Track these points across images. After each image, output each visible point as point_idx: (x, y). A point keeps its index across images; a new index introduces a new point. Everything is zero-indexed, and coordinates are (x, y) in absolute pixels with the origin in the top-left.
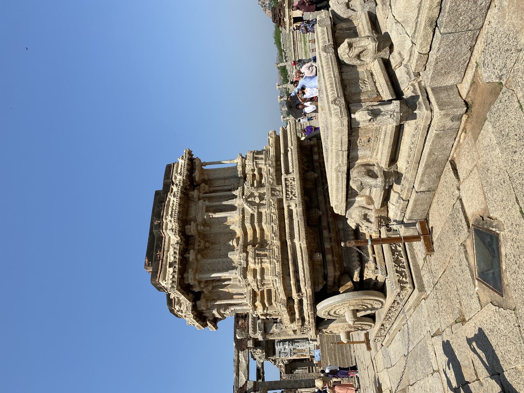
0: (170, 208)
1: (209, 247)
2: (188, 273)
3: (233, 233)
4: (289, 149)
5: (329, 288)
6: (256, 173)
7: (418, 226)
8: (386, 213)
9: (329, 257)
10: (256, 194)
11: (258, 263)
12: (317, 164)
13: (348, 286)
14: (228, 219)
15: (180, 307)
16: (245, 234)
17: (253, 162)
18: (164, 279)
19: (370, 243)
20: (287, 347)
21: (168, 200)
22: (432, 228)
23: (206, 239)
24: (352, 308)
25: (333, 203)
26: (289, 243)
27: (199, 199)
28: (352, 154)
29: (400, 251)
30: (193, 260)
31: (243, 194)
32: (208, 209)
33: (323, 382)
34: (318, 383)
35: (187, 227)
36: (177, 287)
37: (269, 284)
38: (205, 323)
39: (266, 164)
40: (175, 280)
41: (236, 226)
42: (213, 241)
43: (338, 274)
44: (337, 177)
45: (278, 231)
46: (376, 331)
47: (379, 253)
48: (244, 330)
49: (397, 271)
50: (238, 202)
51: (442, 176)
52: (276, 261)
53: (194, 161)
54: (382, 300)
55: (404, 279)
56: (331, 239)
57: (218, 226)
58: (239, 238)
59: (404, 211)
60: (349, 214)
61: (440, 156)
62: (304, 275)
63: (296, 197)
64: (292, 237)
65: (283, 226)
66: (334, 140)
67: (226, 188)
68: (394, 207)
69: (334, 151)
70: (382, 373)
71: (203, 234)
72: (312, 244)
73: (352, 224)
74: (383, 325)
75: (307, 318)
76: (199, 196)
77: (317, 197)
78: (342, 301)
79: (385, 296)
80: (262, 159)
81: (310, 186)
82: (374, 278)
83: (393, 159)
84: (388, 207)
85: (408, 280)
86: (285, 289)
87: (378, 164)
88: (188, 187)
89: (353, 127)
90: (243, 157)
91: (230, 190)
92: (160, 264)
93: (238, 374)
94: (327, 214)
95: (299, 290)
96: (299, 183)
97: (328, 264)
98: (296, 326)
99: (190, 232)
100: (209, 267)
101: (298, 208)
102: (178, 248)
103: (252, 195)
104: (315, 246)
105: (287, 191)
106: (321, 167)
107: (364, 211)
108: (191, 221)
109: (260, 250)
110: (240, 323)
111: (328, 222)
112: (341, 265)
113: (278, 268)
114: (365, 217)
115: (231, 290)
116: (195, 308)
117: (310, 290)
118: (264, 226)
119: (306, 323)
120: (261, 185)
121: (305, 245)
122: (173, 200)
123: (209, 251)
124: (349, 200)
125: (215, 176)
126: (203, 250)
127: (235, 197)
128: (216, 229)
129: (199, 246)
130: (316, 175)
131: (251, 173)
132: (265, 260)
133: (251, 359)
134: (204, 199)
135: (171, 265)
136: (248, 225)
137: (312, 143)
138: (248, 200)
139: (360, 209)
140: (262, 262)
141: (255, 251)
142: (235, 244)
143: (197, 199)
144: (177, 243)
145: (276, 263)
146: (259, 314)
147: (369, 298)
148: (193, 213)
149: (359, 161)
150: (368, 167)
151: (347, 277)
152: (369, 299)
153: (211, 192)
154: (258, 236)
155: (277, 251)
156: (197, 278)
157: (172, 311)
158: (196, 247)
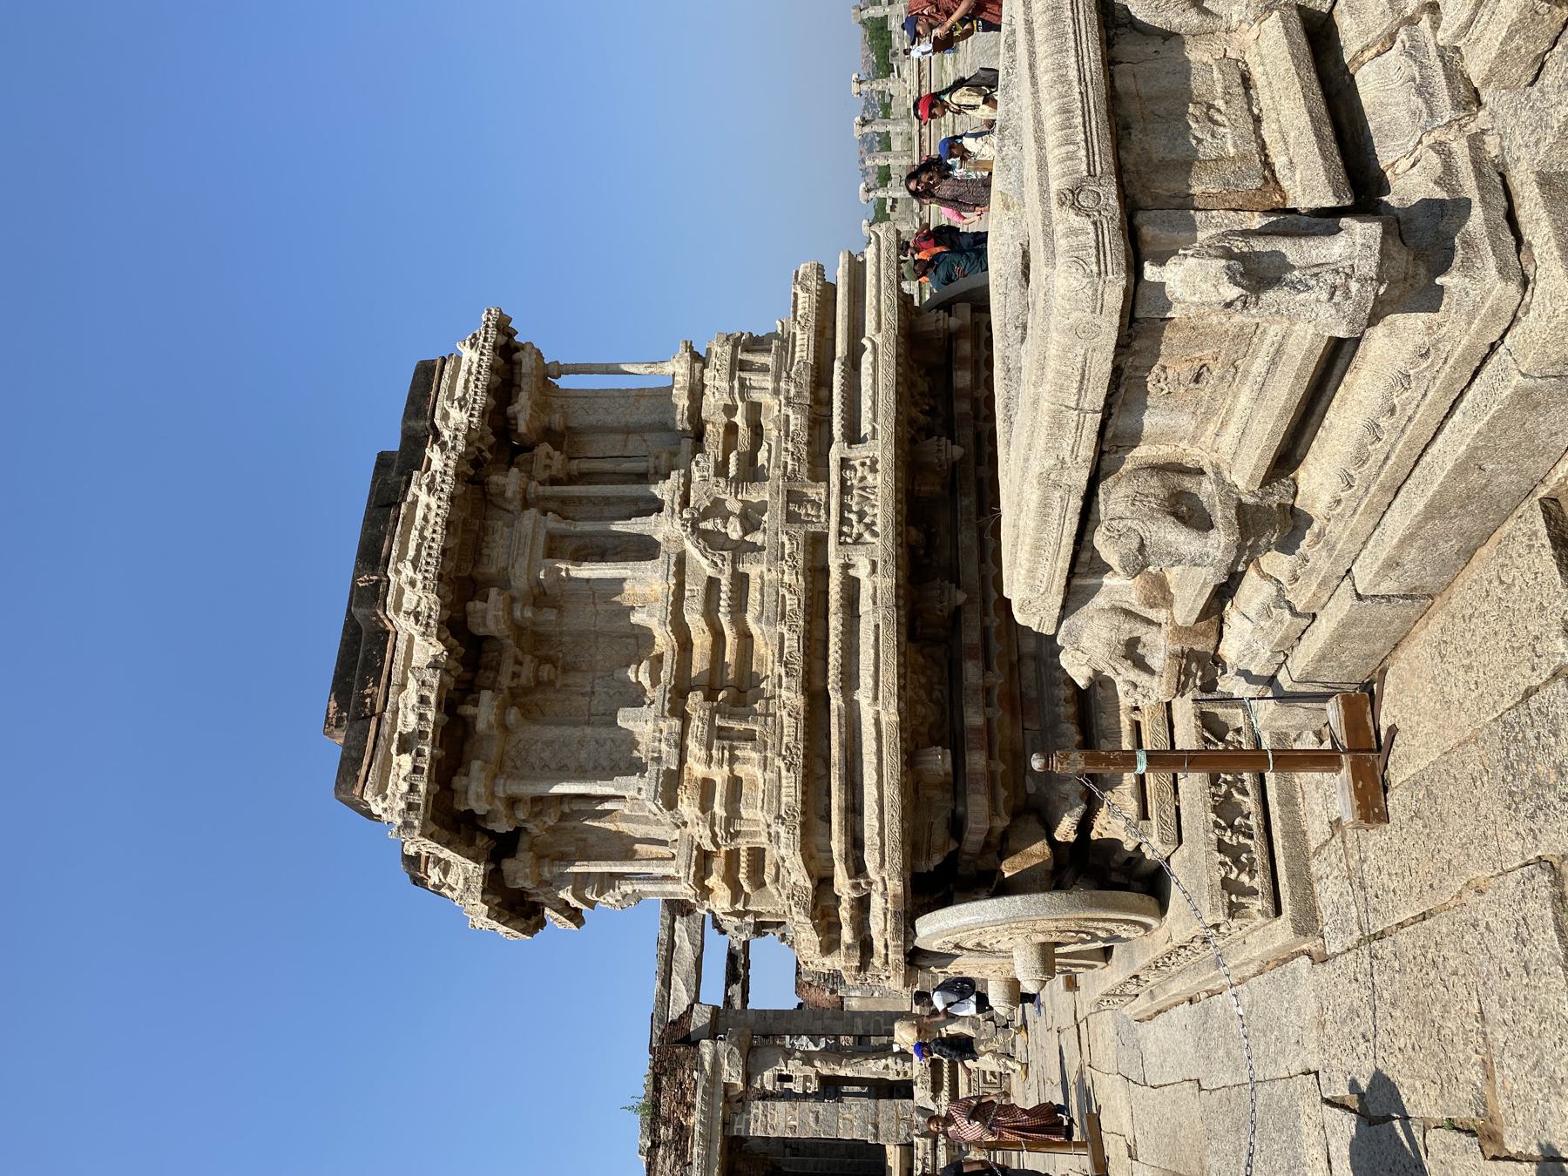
0: (415, 533)
1: (551, 683)
2: (467, 775)
3: (644, 637)
4: (864, 341)
6: (739, 419)
7: (1333, 712)
8: (1213, 642)
9: (977, 760)
10: (733, 505)
11: (721, 765)
12: (963, 406)
13: (1032, 855)
14: (627, 586)
15: (445, 872)
17: (732, 379)
18: (381, 791)
19: (1142, 767)
21: (409, 498)
22: (1393, 731)
23: (543, 652)
24: (1042, 938)
25: (1015, 587)
26: (836, 701)
27: (526, 504)
28: (1120, 422)
30: (490, 727)
31: (685, 502)
32: (555, 547)
33: (919, 1032)
34: (903, 1034)
35: (475, 606)
36: (424, 825)
37: (754, 834)
38: (533, 921)
39: (776, 392)
40: (419, 799)
42: (569, 659)
44: (1045, 504)
45: (799, 656)
49: (1222, 847)
50: (665, 528)
51: (1483, 551)
53: (517, 356)
55: (1244, 878)
56: (988, 691)
57: (590, 608)
58: (659, 659)
59: (1284, 651)
60: (1069, 633)
61: (1504, 478)
62: (882, 828)
63: (875, 534)
64: (850, 680)
66: (1052, 364)
67: (627, 466)
68: (1248, 626)
69: (1045, 405)
70: (1107, 1080)
71: (535, 633)
72: (921, 710)
73: (1076, 667)
75: (878, 945)
76: (525, 491)
77: (954, 531)
78: (1008, 921)
79: (1163, 908)
80: (764, 369)
81: (930, 487)
82: (1129, 846)
83: (1287, 459)
84: (1222, 621)
87: (1218, 473)
88: (488, 455)
89: (1140, 314)
90: (696, 357)
91: (643, 478)
92: (372, 734)
93: (666, 983)
94: (985, 601)
95: (857, 868)
96: (891, 482)
97: (970, 787)
99: (485, 625)
100: (546, 755)
101: (878, 579)
103: (717, 508)
104: (930, 722)
105: (844, 507)
106: (976, 417)
108: (490, 583)
109: (731, 716)
111: (985, 631)
114: (1132, 653)
115: (623, 827)
118: (754, 629)
119: (877, 961)
120: (752, 472)
121: (895, 718)
122: (427, 503)
125: (591, 419)
126: (527, 691)
127: (656, 506)
128: (580, 619)
129: (515, 675)
130: (957, 451)
131: (722, 419)
132: (746, 751)
133: (710, 932)
134: (544, 506)
135: (405, 745)
136: (694, 620)
137: (954, 322)
138: (703, 525)
140: (733, 759)
141: (712, 719)
142: (645, 679)
143: (516, 505)
144: (434, 665)
145: (784, 773)
147: (1104, 916)
148: (497, 556)
149: (1142, 452)
150: (1175, 478)
151: (1033, 825)
152: (1104, 920)
153: (571, 480)
154: (729, 657)
155: (790, 730)
157: (419, 882)
158: (505, 681)
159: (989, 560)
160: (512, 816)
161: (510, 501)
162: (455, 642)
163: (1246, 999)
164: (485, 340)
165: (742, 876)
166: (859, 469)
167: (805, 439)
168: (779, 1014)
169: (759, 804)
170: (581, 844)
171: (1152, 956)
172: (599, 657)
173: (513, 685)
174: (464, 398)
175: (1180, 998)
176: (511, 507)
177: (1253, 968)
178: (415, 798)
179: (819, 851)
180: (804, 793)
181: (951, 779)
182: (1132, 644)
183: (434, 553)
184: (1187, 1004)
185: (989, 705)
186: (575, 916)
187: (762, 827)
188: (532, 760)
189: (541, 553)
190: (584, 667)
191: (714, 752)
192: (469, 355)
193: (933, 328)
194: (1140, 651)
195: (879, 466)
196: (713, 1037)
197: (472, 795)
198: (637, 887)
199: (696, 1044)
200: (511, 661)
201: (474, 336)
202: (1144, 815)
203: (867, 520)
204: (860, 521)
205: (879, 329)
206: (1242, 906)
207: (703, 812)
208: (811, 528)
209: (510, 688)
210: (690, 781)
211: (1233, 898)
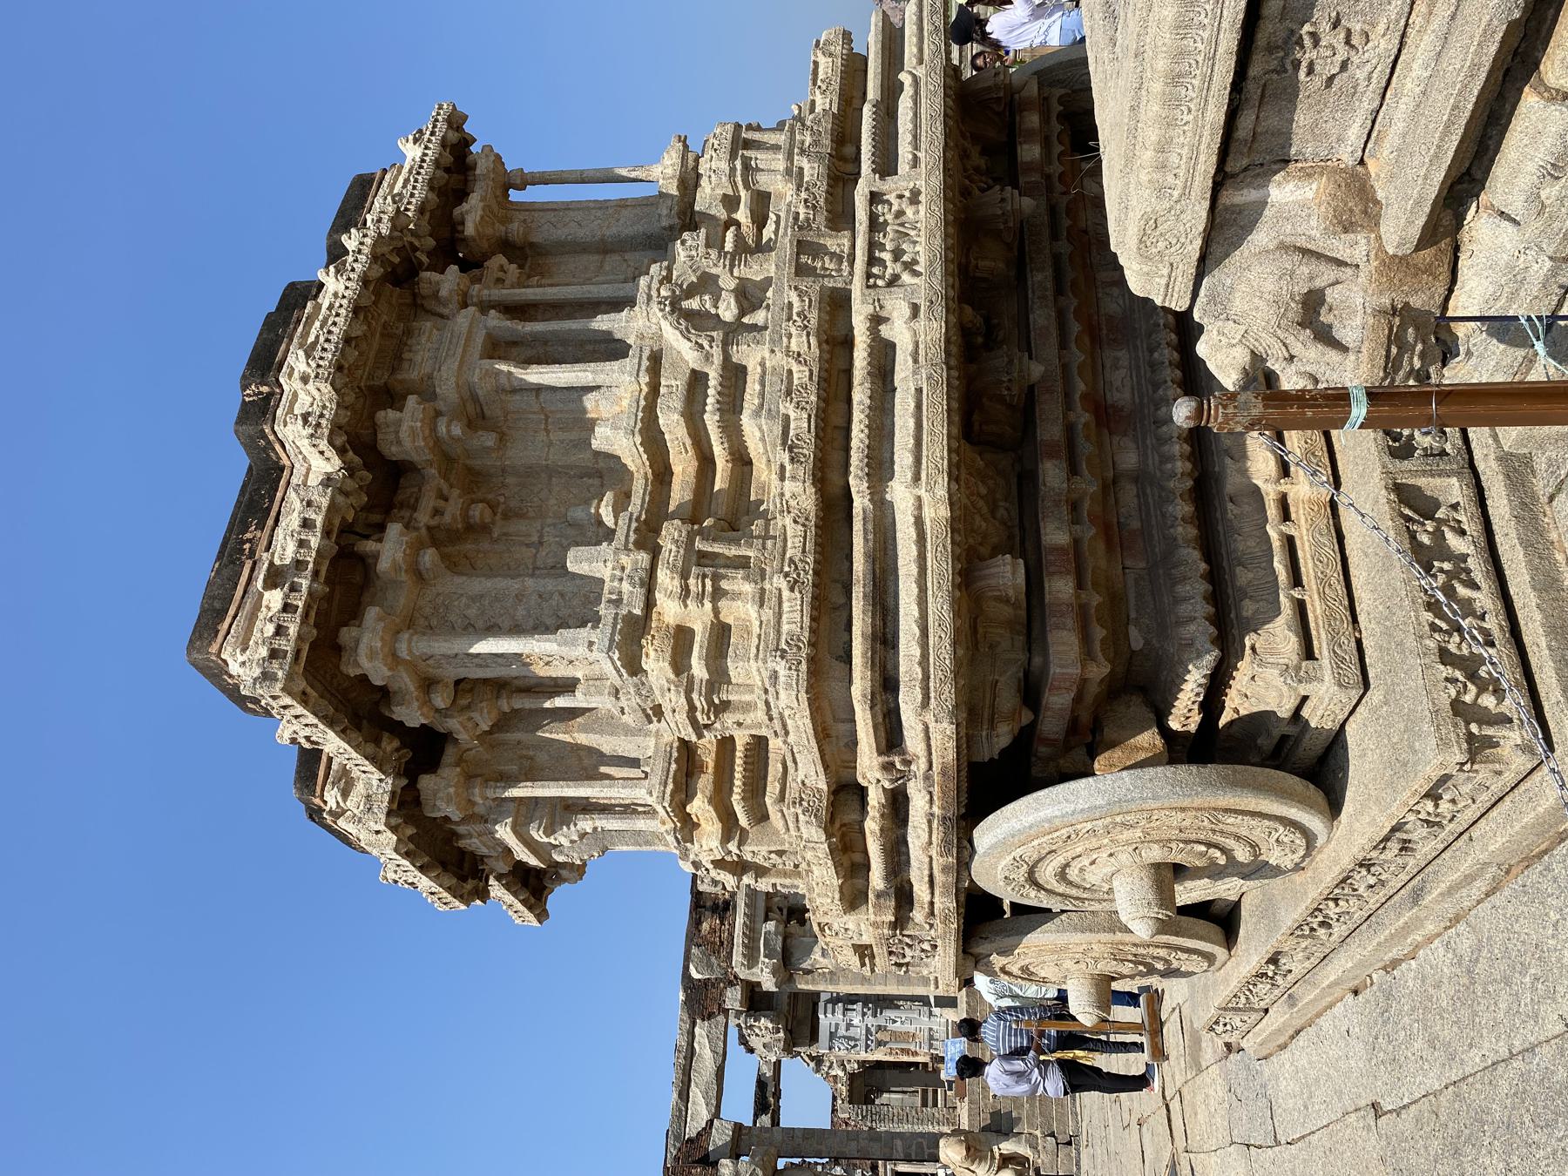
0: (317, 324)
1: (485, 529)
3: (609, 471)
4: (904, 77)
5: (1043, 750)
8: (1441, 291)
9: (1060, 588)
10: (727, 283)
11: (700, 598)
13: (1138, 749)
15: (345, 794)
16: (662, 474)
17: (733, 156)
20: (856, 1022)
24: (1155, 854)
25: (1123, 238)
26: (861, 502)
27: (465, 305)
29: (1464, 558)
30: (396, 567)
32: (498, 348)
33: (968, 1149)
36: (290, 677)
37: (747, 707)
39: (788, 172)
41: (615, 428)
42: (513, 504)
43: (1099, 671)
45: (810, 438)
46: (1234, 985)
47: (1323, 581)
48: (716, 952)
49: (1445, 656)
52: (784, 585)
54: (1314, 822)
55: (1488, 701)
56: (1075, 507)
57: (542, 436)
60: (1212, 299)
63: (916, 274)
64: (880, 468)
71: (469, 469)
74: (1274, 960)
75: (921, 891)
79: (1334, 806)
81: (992, 262)
82: (1285, 711)
84: (1457, 249)
85: (1513, 703)
86: (823, 734)
88: (424, 259)
93: (684, 1095)
94: (1068, 396)
96: (938, 210)
97: (1051, 621)
98: (868, 924)
99: (399, 442)
100: (472, 612)
102: (325, 502)
103: (707, 284)
105: (872, 245)
107: (1307, 275)
110: (705, 926)
111: (1070, 429)
112: (1117, 637)
113: (795, 615)
116: (406, 809)
117: (950, 729)
119: (918, 915)
121: (944, 512)
123: (486, 545)
125: (561, 233)
128: (527, 450)
129: (437, 512)
132: (737, 583)
134: (484, 307)
135: (275, 577)
138: (685, 304)
139: (1289, 261)
140: (718, 594)
143: (453, 306)
144: (328, 481)
145: (786, 594)
146: (706, 860)
151: (1136, 707)
152: (1253, 814)
156: (403, 653)
157: (315, 814)
158: (423, 517)
159: (1073, 346)
160: (427, 702)
162: (357, 459)
163: (1465, 945)
164: (433, 134)
165: (736, 798)
166: (895, 202)
167: (824, 188)
168: (809, 1133)
169: (754, 650)
170: (527, 763)
171: (1314, 894)
172: (553, 501)
174: (400, 194)
175: (1338, 992)
176: (445, 311)
177: (1481, 886)
179: (836, 720)
180: (813, 619)
181: (1023, 613)
182: (1313, 302)
183: (334, 338)
184: (1350, 997)
185: (1076, 521)
187: (759, 692)
188: (453, 618)
190: (531, 514)
191: (692, 581)
192: (412, 152)
193: (990, 83)
194: (1325, 317)
195: (922, 198)
196: (736, 1156)
197: (363, 650)
199: (715, 1164)
201: (420, 131)
202: (1308, 653)
203: (905, 258)
204: (896, 259)
205: (921, 61)
206: (1491, 743)
207: (678, 673)
208: (829, 283)
209: (429, 528)
210: (658, 629)
211: (1474, 728)
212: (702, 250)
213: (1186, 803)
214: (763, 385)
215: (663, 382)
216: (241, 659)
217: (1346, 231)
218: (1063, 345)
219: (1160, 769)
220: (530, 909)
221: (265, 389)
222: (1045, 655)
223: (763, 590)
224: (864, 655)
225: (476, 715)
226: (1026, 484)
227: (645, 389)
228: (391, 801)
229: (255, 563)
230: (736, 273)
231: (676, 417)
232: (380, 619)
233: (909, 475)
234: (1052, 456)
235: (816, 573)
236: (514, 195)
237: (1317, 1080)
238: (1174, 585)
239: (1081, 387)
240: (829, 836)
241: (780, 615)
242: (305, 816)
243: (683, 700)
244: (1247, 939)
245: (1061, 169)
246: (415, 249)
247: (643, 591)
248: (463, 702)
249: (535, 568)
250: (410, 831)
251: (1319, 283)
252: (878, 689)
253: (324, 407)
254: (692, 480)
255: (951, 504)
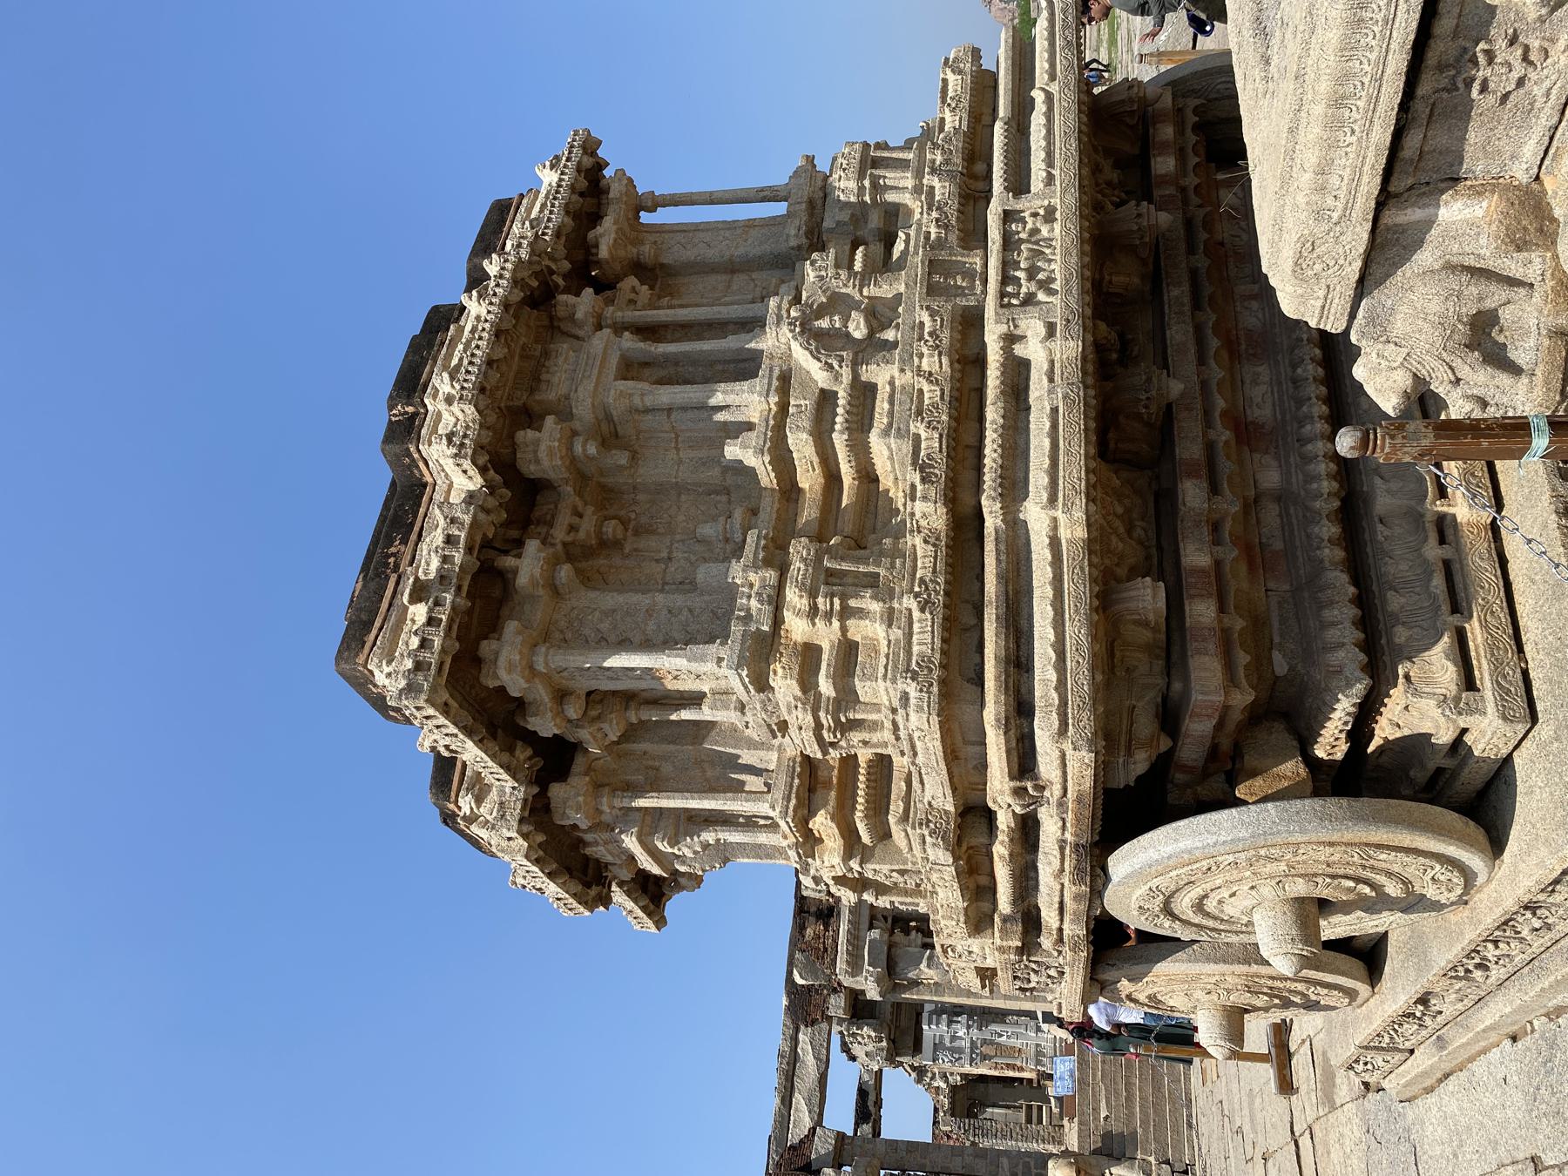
0: (461, 347)
1: (617, 544)
4: (1039, 96)
5: (1180, 777)
9: (1202, 611)
11: (828, 616)
15: (479, 800)
17: (861, 177)
24: (1300, 888)
25: (1277, 259)
26: (993, 520)
27: (599, 327)
30: (534, 582)
35: (525, 436)
36: (434, 689)
37: (875, 726)
38: (594, 891)
39: (917, 190)
40: (432, 658)
42: (643, 520)
43: (1243, 698)
45: (941, 460)
46: (1377, 1024)
52: (914, 606)
54: (1474, 861)
56: (1216, 527)
57: (672, 454)
60: (1372, 320)
64: (1014, 488)
65: (972, 441)
71: (604, 488)
74: (1423, 1000)
75: (1049, 916)
79: (1496, 843)
81: (1126, 277)
86: (952, 756)
88: (561, 282)
92: (388, 593)
95: (1024, 762)
96: (1074, 229)
97: (1192, 646)
99: (537, 461)
100: (605, 626)
101: (1057, 344)
102: (467, 519)
103: (837, 303)
105: (1007, 265)
107: (1476, 296)
110: (809, 932)
111: (1210, 447)
112: (1261, 662)
113: (925, 637)
116: (537, 816)
117: (1088, 757)
119: (1046, 942)
121: (1081, 533)
123: (617, 561)
124: (1393, 217)
125: (690, 254)
128: (659, 467)
129: (572, 528)
134: (619, 328)
136: (801, 444)
139: (1453, 282)
140: (846, 613)
143: (588, 328)
144: (471, 497)
145: (916, 614)
146: (827, 876)
148: (558, 381)
151: (1278, 735)
155: (924, 556)
156: (541, 667)
157: (449, 819)
158: (559, 534)
160: (560, 713)
161: (580, 325)
162: (498, 478)
164: (568, 159)
167: (956, 206)
168: (912, 1146)
169: (881, 670)
170: (651, 773)
171: (1471, 935)
172: (681, 518)
173: (569, 539)
176: (581, 333)
178: (426, 655)
179: (966, 742)
180: (944, 641)
181: (1163, 637)
183: (477, 361)
184: (1507, 1043)
186: (652, 893)
188: (587, 631)
189: (612, 377)
190: (661, 530)
191: (820, 600)
192: (549, 178)
196: (838, 1166)
197: (502, 662)
198: (721, 836)
200: (569, 512)
202: (1469, 682)
204: (1031, 278)
205: (1053, 77)
207: (804, 690)
209: (565, 544)
212: (831, 271)
213: (1335, 837)
214: (891, 403)
215: (792, 402)
216: (387, 670)
217: (1519, 249)
218: (1202, 360)
219: (1307, 802)
220: (649, 915)
221: (410, 409)
222: (1186, 679)
223: (891, 610)
224: (997, 678)
225: (606, 726)
226: (1164, 504)
227: (774, 408)
228: (523, 809)
229: (399, 577)
230: (865, 293)
231: (805, 436)
232: (519, 633)
233: (1045, 496)
234: (1191, 474)
235: (947, 593)
236: (645, 218)
237: (1469, 1128)
238: (1321, 608)
239: (1220, 404)
240: (956, 859)
241: (911, 634)
242: (439, 820)
243: (810, 718)
244: (1394, 977)
245: (1197, 181)
246: (552, 272)
247: (771, 608)
248: (594, 713)
249: (665, 583)
250: (541, 838)
251: (1489, 304)
252: (1013, 713)
253: (467, 427)
254: (819, 497)
255: (1089, 525)
